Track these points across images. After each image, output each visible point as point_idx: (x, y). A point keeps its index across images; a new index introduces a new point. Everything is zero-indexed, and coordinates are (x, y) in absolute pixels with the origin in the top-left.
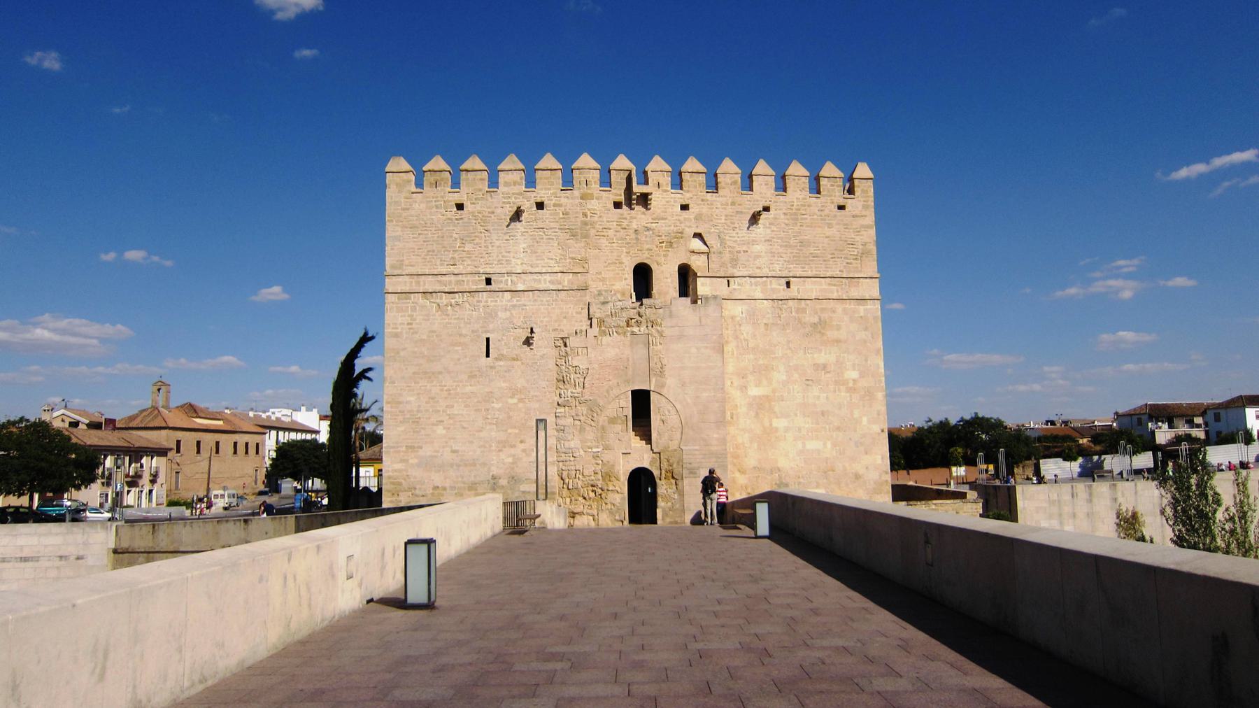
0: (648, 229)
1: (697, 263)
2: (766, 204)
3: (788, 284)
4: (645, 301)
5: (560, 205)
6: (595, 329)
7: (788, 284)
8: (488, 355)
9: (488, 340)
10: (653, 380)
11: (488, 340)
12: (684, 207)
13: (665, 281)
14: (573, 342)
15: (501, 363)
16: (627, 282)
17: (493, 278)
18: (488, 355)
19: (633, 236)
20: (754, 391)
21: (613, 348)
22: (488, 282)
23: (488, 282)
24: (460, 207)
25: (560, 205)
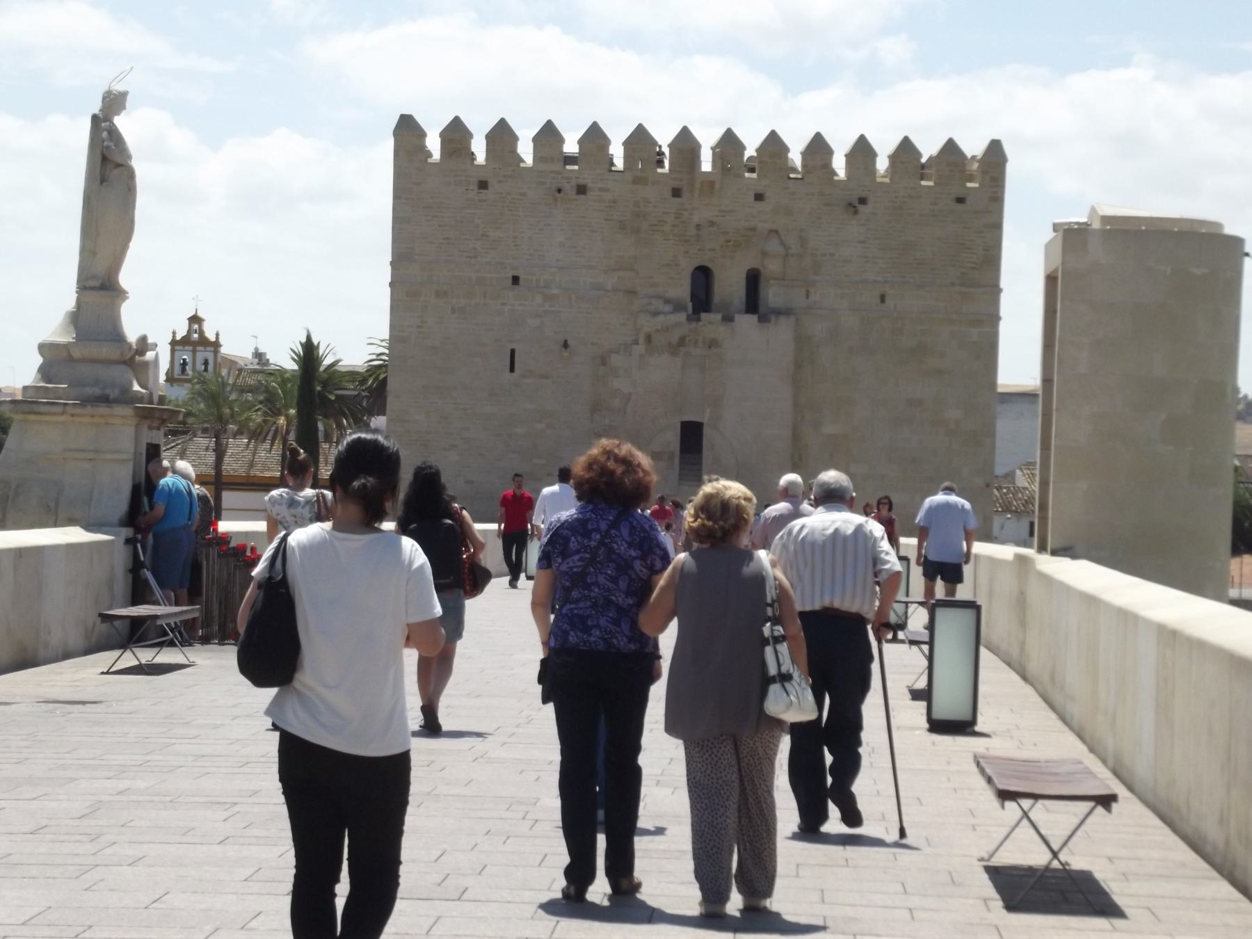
0: (712, 224)
1: (772, 267)
2: (864, 194)
3: (883, 299)
4: (703, 315)
5: (607, 190)
6: (640, 348)
7: (883, 299)
8: (512, 369)
9: (513, 351)
10: (708, 410)
11: (513, 351)
12: (759, 197)
13: (730, 284)
14: (616, 360)
15: (528, 381)
16: (682, 290)
17: (522, 277)
18: (512, 369)
19: (692, 231)
20: (828, 429)
21: (662, 371)
22: (516, 280)
23: (516, 280)
24: (483, 185)
25: (607, 190)
